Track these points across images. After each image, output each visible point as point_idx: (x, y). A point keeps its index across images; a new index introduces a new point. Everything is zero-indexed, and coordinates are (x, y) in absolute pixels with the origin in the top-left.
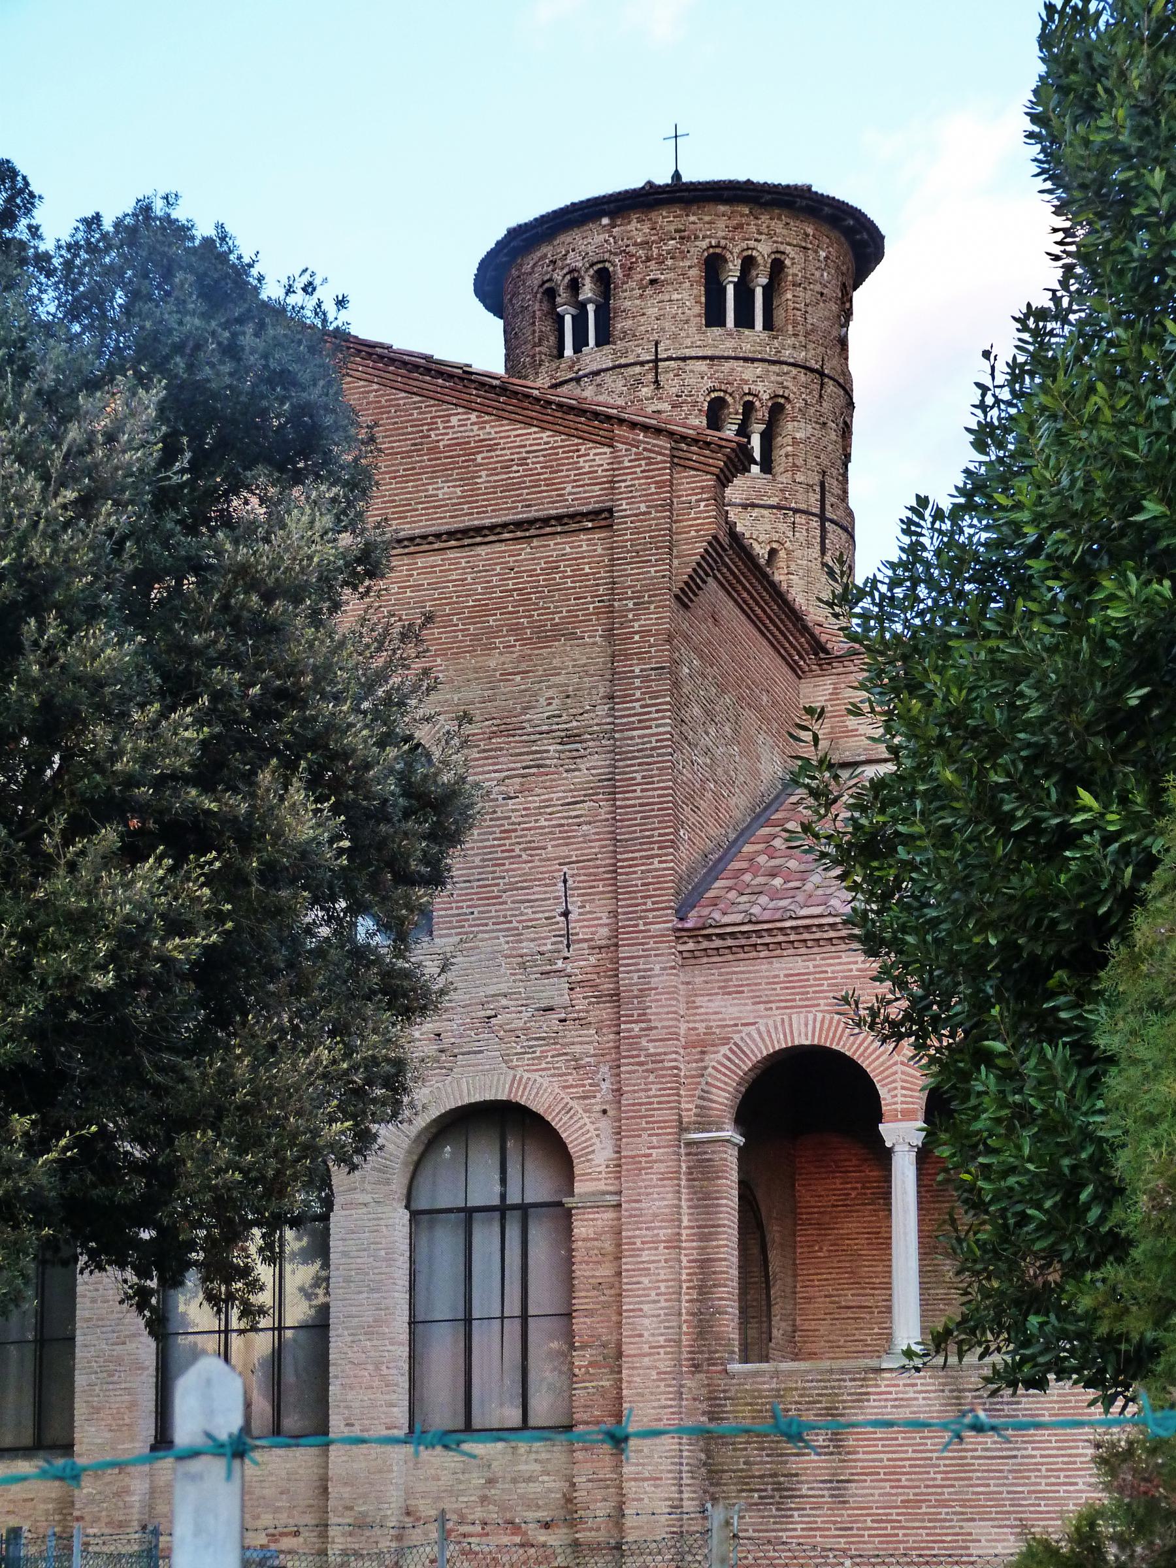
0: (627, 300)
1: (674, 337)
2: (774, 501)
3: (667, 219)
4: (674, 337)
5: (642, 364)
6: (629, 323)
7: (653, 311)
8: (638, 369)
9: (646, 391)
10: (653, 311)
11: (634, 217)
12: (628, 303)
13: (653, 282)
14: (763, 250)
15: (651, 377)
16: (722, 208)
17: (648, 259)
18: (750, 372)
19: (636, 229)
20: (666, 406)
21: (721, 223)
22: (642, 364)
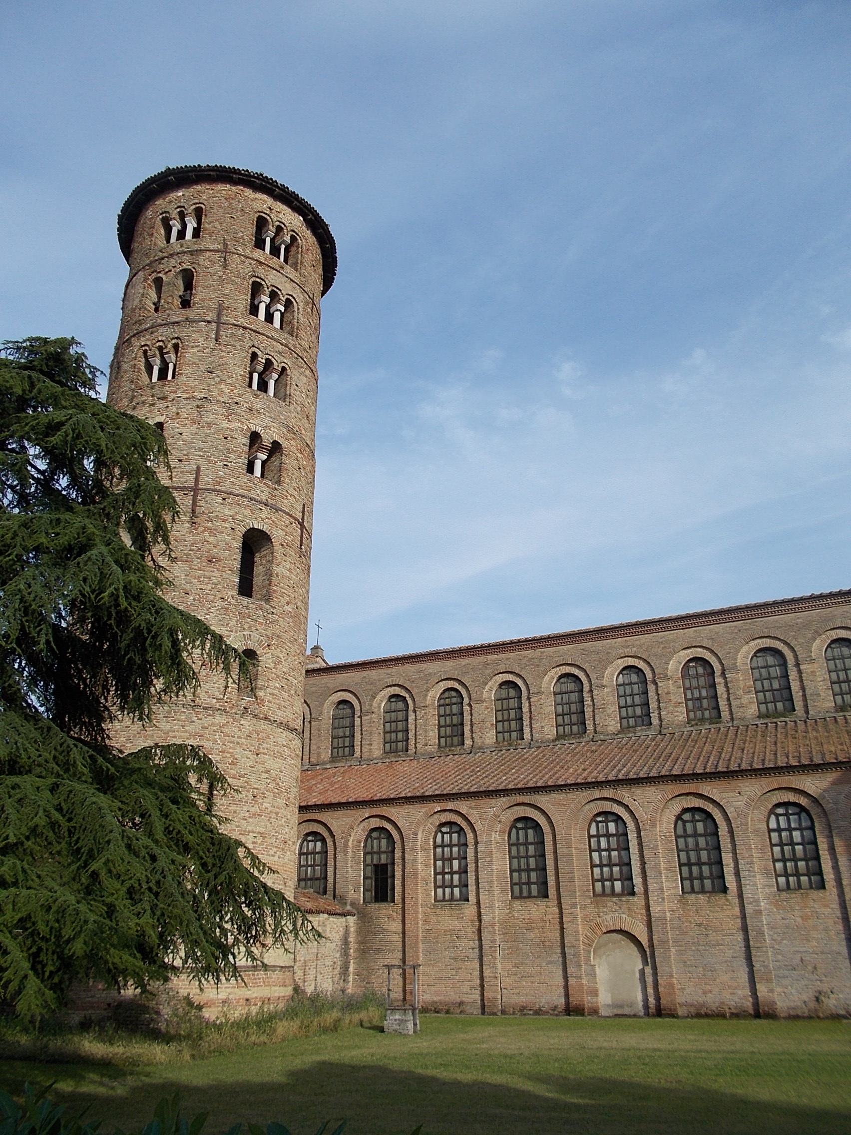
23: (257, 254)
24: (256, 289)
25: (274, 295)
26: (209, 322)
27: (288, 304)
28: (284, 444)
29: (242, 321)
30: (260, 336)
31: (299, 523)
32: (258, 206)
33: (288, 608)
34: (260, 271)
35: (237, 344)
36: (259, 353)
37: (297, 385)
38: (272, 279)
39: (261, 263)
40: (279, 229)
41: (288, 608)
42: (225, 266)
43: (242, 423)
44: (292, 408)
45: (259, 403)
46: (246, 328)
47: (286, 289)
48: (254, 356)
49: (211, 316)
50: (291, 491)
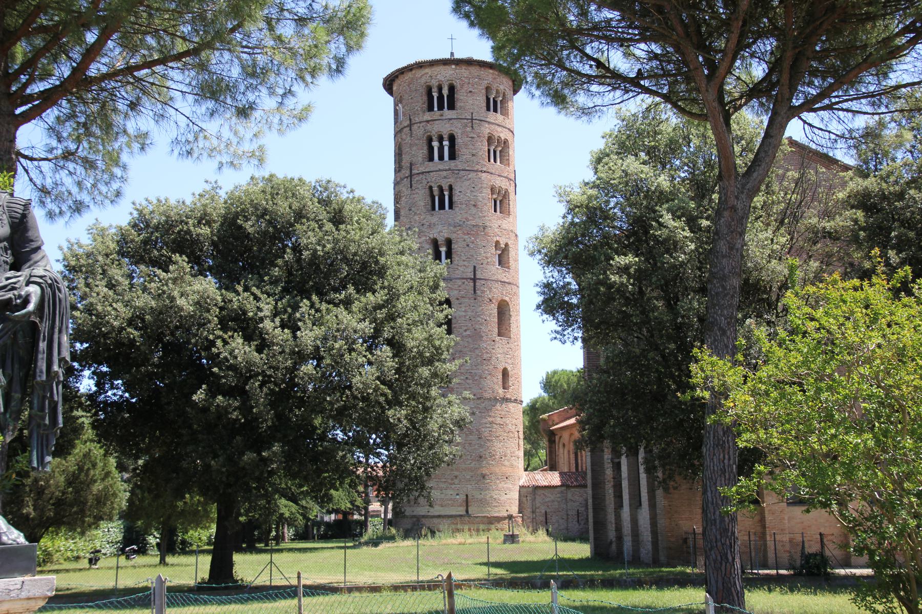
0: (461, 96)
1: (478, 112)
2: (506, 175)
3: (474, 70)
4: (478, 112)
5: (467, 119)
6: (462, 104)
7: (471, 102)
8: (466, 121)
9: (469, 129)
10: (471, 102)
11: (463, 67)
12: (462, 98)
13: (470, 92)
14: (502, 87)
15: (470, 124)
16: (491, 71)
17: (469, 83)
18: (499, 129)
19: (464, 71)
20: (475, 136)
21: (491, 76)
22: (467, 119)
23: (428, 116)
24: (430, 140)
25: (441, 139)
26: (407, 177)
27: (452, 139)
28: (453, 236)
29: (422, 169)
30: (432, 174)
31: (471, 279)
32: (423, 80)
33: (468, 333)
34: (429, 127)
35: (419, 186)
36: (433, 185)
37: (460, 192)
38: (436, 129)
39: (428, 121)
40: (440, 89)
41: (468, 333)
42: (411, 136)
43: (426, 236)
44: (457, 209)
45: (434, 219)
46: (423, 173)
47: (445, 129)
48: (431, 188)
49: (408, 173)
50: (461, 263)
